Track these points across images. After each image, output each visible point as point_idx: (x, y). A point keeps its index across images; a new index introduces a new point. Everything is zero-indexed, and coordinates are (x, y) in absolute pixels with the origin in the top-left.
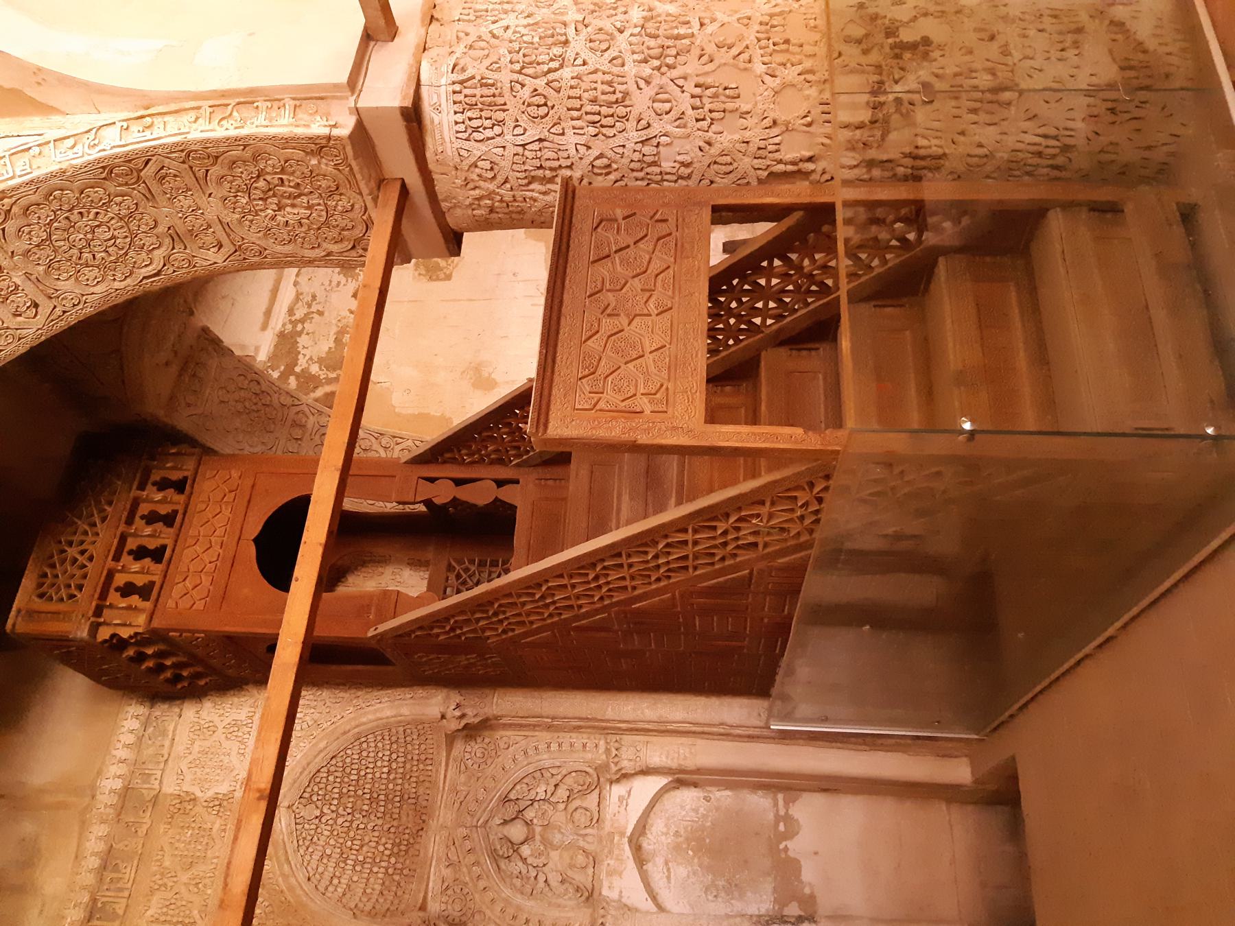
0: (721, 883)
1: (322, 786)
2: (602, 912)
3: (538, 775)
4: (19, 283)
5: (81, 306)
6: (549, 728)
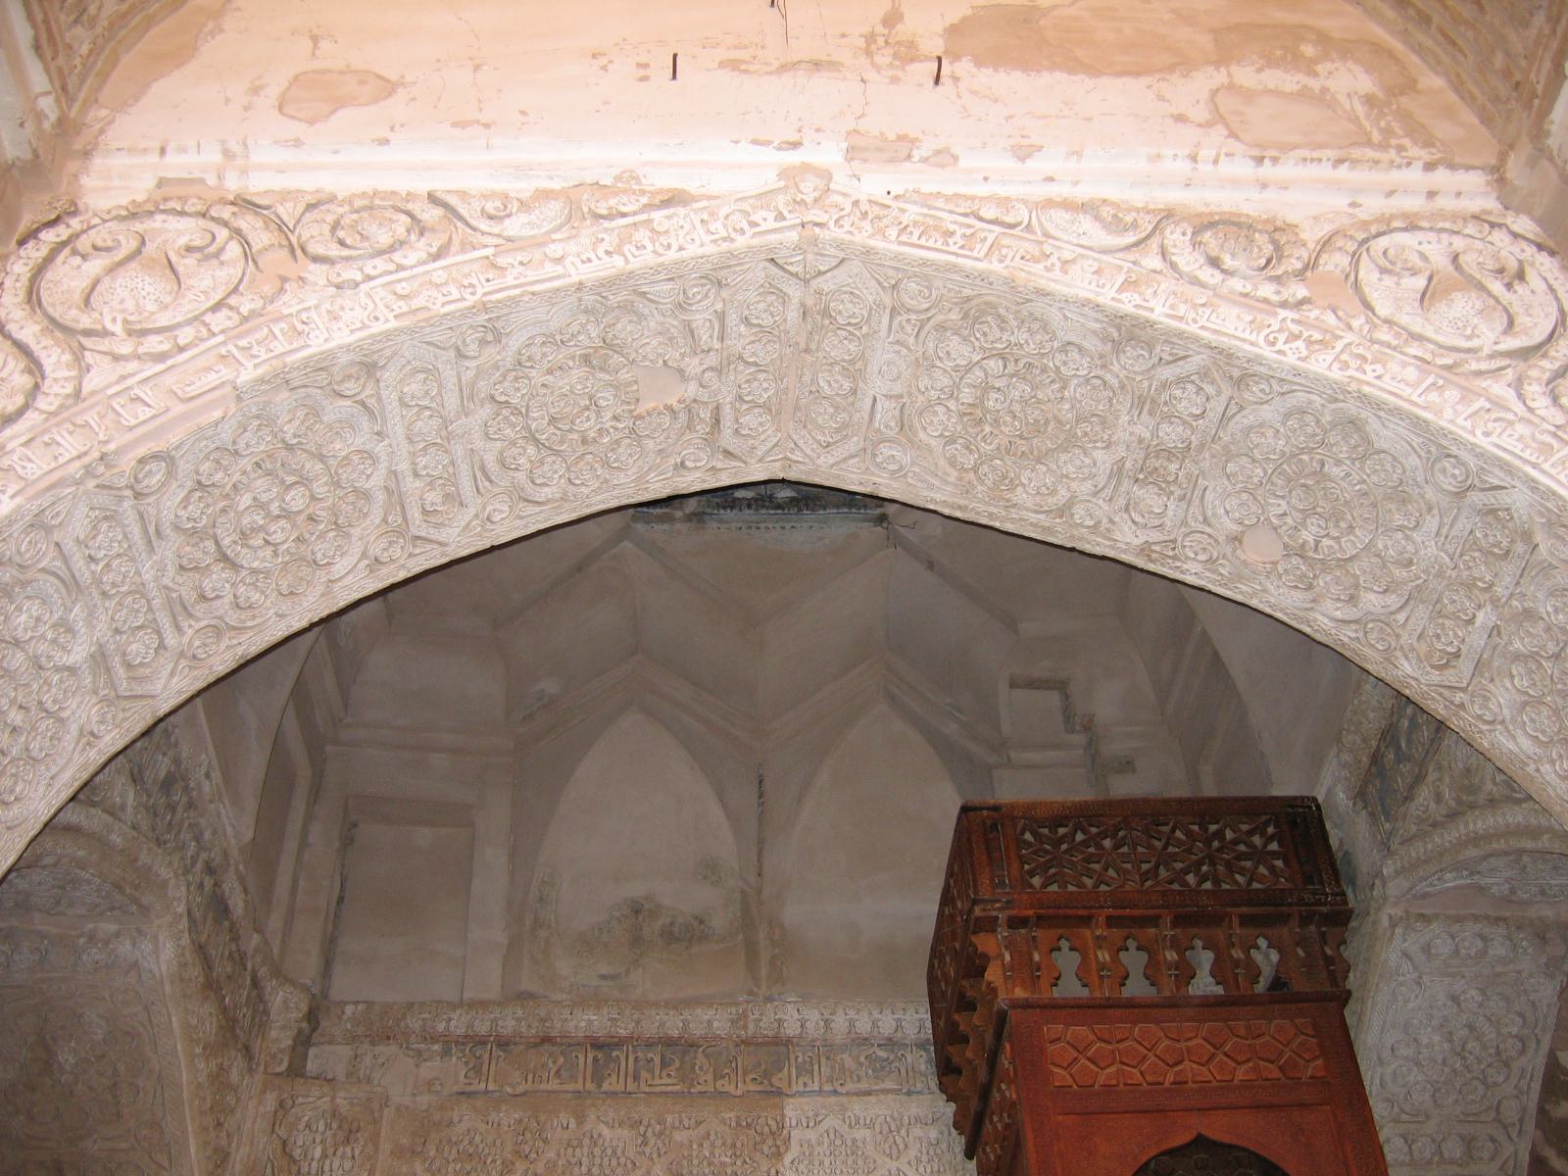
4: (1479, 621)
5: (1485, 727)
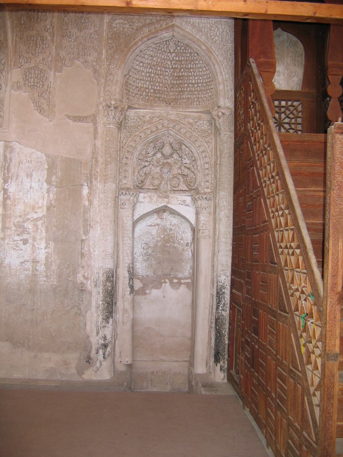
0: (150, 251)
1: (184, 51)
2: (131, 193)
3: (194, 159)
6: (216, 163)
